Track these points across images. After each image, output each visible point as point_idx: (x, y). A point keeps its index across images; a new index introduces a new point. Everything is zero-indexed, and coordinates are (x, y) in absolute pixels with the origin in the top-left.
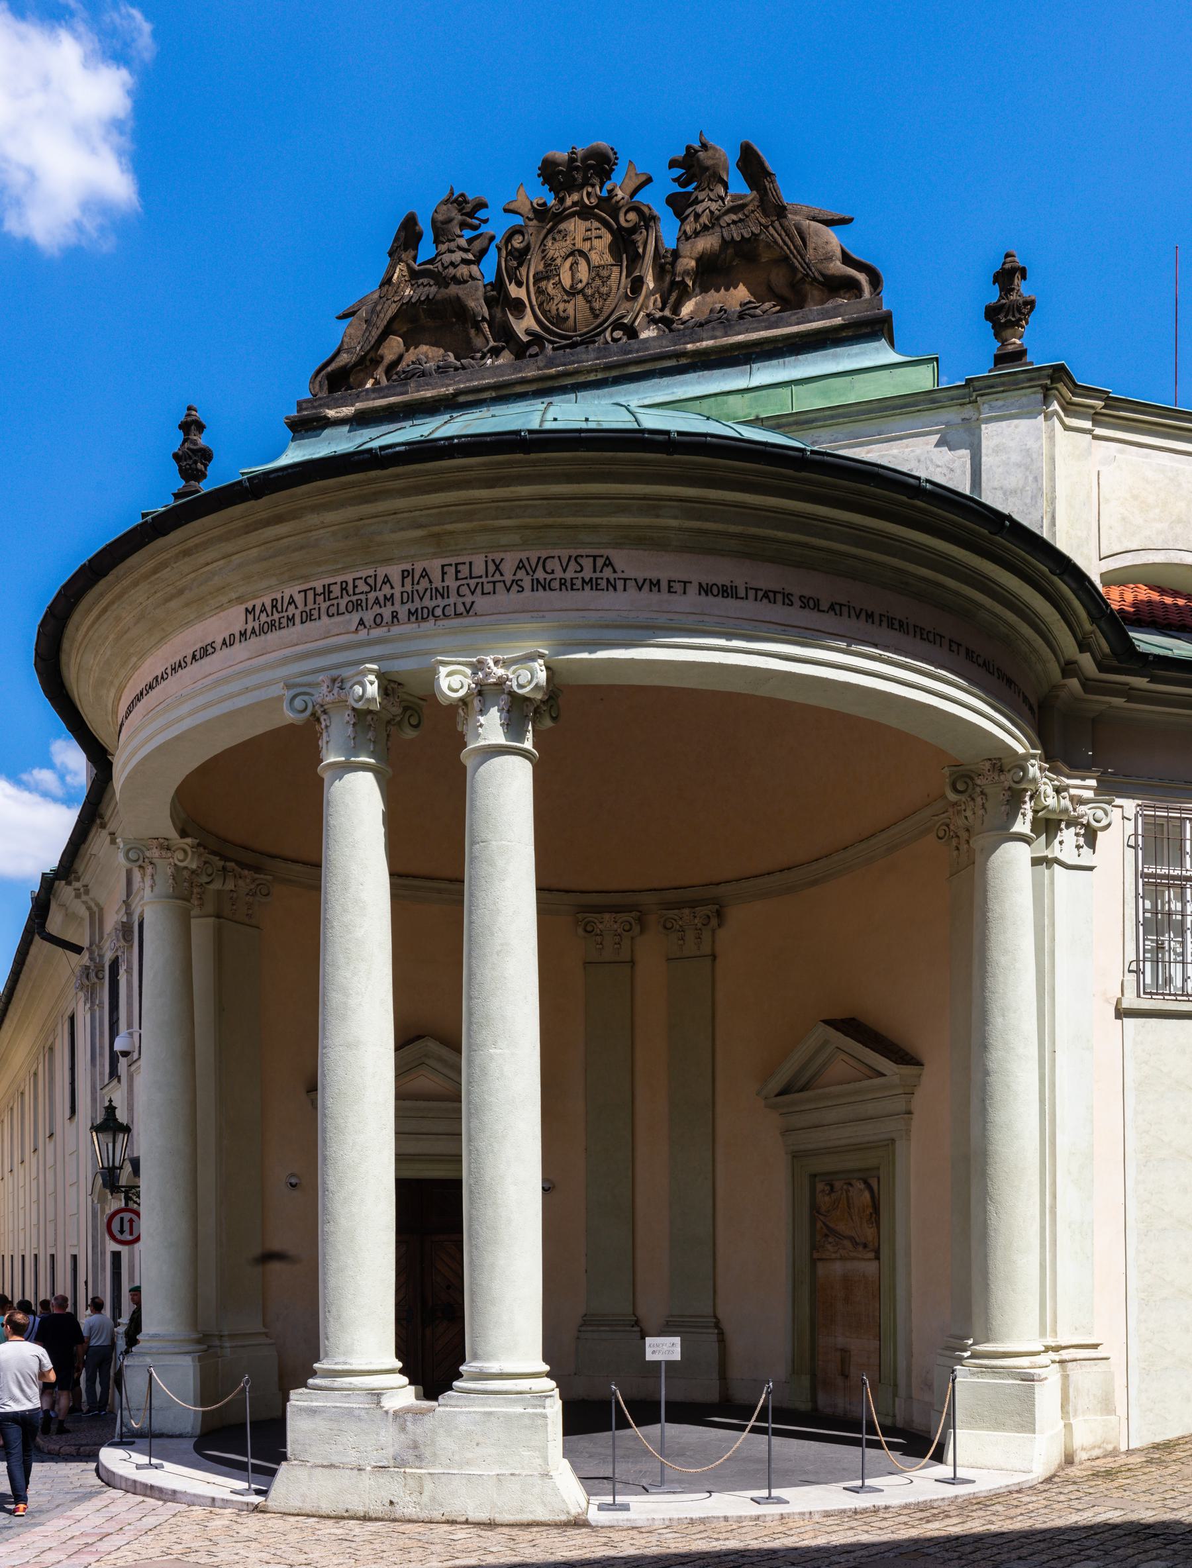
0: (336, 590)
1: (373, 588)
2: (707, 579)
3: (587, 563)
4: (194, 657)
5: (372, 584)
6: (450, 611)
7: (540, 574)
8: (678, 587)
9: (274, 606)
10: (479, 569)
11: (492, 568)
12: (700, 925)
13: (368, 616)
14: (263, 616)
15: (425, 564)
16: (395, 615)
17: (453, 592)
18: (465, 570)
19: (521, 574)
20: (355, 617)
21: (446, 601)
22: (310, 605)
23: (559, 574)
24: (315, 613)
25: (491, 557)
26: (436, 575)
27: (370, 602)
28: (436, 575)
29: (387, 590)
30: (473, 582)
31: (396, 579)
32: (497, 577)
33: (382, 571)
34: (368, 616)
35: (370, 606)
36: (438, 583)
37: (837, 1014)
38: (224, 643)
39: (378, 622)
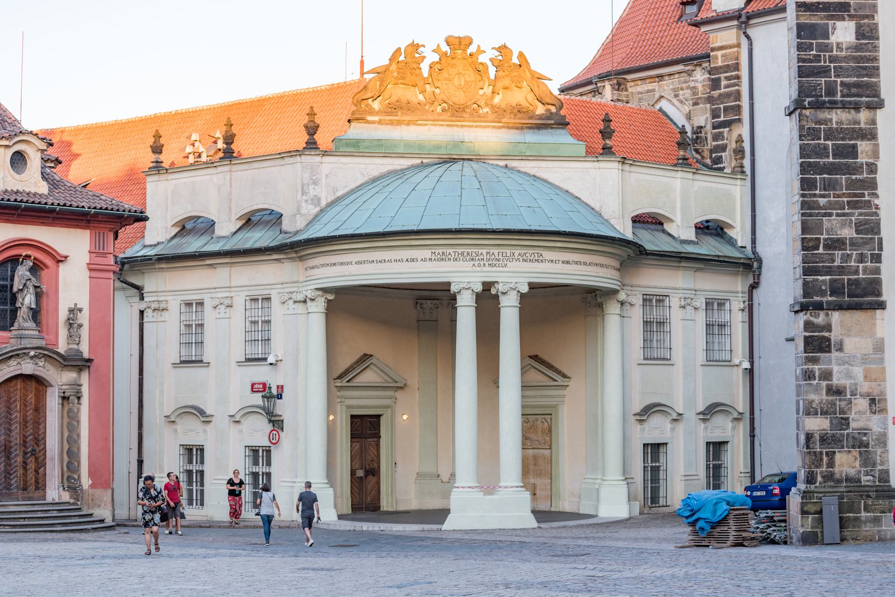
0: (465, 254)
1: (477, 255)
2: (564, 260)
3: (536, 255)
4: (407, 260)
8: (557, 262)
9: (443, 254)
10: (508, 254)
11: (512, 255)
13: (476, 263)
14: (439, 256)
16: (484, 265)
17: (501, 260)
18: (504, 255)
19: (520, 257)
20: (472, 263)
21: (499, 263)
23: (529, 258)
24: (458, 260)
26: (496, 254)
28: (496, 254)
29: (482, 256)
30: (507, 258)
31: (485, 254)
32: (513, 257)
33: (480, 251)
34: (476, 263)
36: (497, 257)
37: (532, 354)
38: (422, 260)
39: (479, 265)
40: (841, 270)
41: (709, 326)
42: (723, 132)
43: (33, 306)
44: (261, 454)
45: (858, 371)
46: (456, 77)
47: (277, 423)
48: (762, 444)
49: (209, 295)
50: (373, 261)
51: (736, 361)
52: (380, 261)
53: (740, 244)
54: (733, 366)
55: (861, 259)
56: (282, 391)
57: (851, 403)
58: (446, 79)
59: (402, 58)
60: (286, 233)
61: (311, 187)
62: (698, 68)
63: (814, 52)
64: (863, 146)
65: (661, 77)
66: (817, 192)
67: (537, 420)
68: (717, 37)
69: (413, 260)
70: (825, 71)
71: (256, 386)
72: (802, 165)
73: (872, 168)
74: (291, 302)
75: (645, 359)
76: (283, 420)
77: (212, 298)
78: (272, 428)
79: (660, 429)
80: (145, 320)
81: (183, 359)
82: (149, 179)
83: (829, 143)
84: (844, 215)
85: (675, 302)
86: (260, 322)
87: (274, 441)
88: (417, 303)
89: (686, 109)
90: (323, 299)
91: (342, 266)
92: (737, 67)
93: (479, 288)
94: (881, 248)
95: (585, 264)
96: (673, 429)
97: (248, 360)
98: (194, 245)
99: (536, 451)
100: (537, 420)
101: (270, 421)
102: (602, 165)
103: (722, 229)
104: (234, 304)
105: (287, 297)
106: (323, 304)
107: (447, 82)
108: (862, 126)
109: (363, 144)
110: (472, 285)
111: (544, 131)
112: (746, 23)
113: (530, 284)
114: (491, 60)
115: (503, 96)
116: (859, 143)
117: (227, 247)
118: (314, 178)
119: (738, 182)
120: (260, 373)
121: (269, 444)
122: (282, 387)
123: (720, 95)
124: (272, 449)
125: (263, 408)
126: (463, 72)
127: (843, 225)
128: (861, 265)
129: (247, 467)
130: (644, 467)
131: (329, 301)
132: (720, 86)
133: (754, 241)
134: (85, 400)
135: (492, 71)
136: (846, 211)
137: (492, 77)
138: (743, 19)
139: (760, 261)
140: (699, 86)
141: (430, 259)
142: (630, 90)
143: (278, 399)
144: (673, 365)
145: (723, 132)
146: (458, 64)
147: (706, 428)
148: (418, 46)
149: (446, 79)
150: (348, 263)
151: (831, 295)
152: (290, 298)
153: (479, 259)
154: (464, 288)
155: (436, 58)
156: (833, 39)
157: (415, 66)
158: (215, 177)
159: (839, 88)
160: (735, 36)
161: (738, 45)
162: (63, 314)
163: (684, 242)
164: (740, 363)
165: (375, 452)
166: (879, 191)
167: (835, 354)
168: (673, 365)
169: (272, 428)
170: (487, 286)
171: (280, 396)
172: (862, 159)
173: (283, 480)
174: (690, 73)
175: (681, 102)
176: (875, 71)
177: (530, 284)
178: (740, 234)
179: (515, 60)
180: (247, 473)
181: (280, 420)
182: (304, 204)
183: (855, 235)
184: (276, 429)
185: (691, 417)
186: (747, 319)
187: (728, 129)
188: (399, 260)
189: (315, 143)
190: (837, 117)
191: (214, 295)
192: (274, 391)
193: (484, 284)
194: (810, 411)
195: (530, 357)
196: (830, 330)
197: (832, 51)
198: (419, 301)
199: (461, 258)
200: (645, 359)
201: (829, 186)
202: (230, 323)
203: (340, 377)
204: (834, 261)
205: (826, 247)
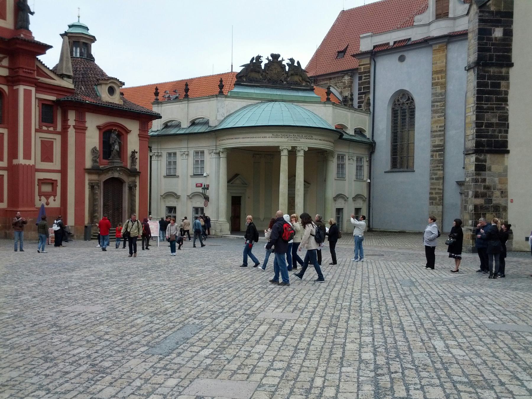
39: (290, 140)
40: (492, 136)
41: (357, 166)
43: (118, 150)
45: (496, 179)
47: (207, 198)
51: (365, 179)
53: (368, 137)
55: (500, 132)
57: (493, 193)
58: (271, 70)
59: (254, 61)
60: (211, 127)
62: (346, 75)
63: (485, 41)
64: (503, 83)
65: (330, 79)
66: (483, 102)
70: (489, 50)
72: (477, 90)
73: (506, 93)
74: (213, 154)
75: (337, 178)
80: (152, 159)
81: (168, 174)
82: (153, 106)
83: (489, 81)
84: (493, 113)
85: (347, 157)
89: (340, 90)
92: (369, 72)
93: (290, 149)
94: (508, 127)
95: (326, 141)
96: (345, 203)
98: (173, 131)
102: (327, 105)
103: (361, 132)
105: (211, 151)
108: (503, 74)
110: (287, 148)
111: (305, 92)
112: (374, 55)
113: (308, 148)
114: (287, 64)
116: (501, 82)
117: (187, 132)
119: (368, 115)
120: (200, 180)
122: (209, 185)
123: (362, 82)
125: (202, 193)
127: (493, 117)
128: (500, 134)
133: (373, 136)
134: (138, 188)
135: (287, 68)
136: (495, 111)
137: (287, 70)
138: (373, 53)
139: (375, 143)
140: (346, 81)
142: (318, 83)
147: (355, 203)
148: (260, 57)
150: (238, 138)
151: (487, 147)
152: (213, 152)
154: (284, 149)
155: (267, 62)
156: (493, 36)
157: (259, 64)
159: (495, 57)
161: (370, 64)
162: (129, 153)
163: (351, 135)
164: (367, 180)
166: (509, 103)
167: (487, 172)
170: (294, 148)
172: (503, 89)
174: (343, 77)
175: (338, 87)
176: (510, 50)
177: (308, 148)
178: (368, 134)
179: (296, 64)
182: (218, 116)
183: (498, 122)
185: (350, 199)
186: (368, 165)
189: (223, 92)
190: (492, 70)
191: (181, 150)
193: (292, 147)
194: (476, 195)
196: (486, 162)
197: (492, 41)
200: (337, 178)
201: (488, 100)
204: (489, 132)
205: (486, 126)
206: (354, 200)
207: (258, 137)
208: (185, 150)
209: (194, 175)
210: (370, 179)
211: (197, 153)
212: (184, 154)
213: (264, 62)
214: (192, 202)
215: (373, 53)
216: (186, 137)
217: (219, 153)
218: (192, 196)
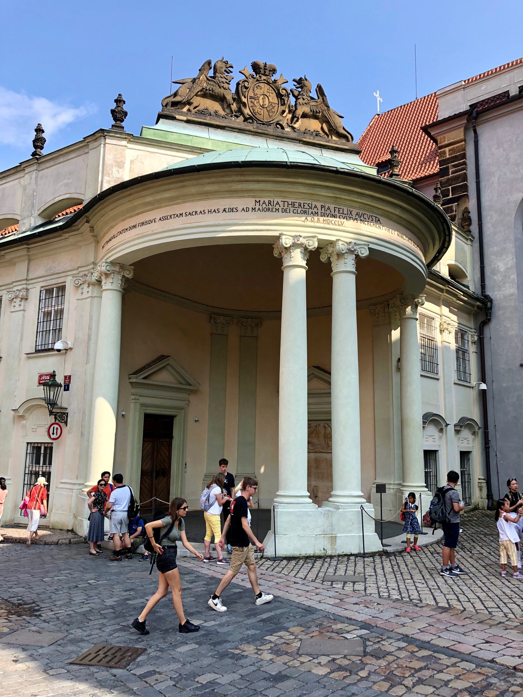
0: (297, 205)
1: (311, 208)
3: (374, 218)
4: (224, 210)
5: (311, 206)
6: (336, 223)
7: (362, 218)
9: (270, 203)
10: (345, 212)
12: (254, 325)
14: (264, 206)
15: (329, 205)
18: (341, 211)
19: (357, 217)
22: (286, 207)
24: (288, 211)
25: (349, 209)
27: (310, 213)
28: (333, 210)
30: (344, 215)
31: (319, 208)
32: (351, 216)
33: (314, 203)
35: (310, 213)
36: (333, 213)
38: (243, 209)
42: (452, 206)
44: (42, 452)
46: (262, 97)
48: (498, 454)
49: (5, 292)
50: (181, 215)
52: (190, 214)
54: (470, 387)
56: (70, 382)
61: (114, 169)
67: (319, 425)
68: (444, 138)
69: (232, 210)
71: (43, 378)
74: (86, 285)
76: (67, 413)
77: (8, 292)
78: (53, 421)
79: (433, 437)
86: (53, 311)
87: (55, 436)
88: (211, 317)
90: (120, 277)
91: (144, 227)
92: (464, 156)
93: (314, 245)
96: (440, 438)
97: (37, 351)
99: (318, 454)
100: (319, 425)
101: (51, 413)
104: (30, 297)
106: (120, 282)
107: (253, 100)
109: (171, 136)
112: (476, 118)
115: (302, 123)
118: (118, 160)
119: (469, 242)
121: (49, 441)
122: (70, 377)
123: (448, 179)
124: (54, 446)
126: (268, 95)
129: (27, 466)
130: (425, 472)
131: (125, 280)
132: (449, 172)
133: (483, 287)
135: (292, 100)
138: (474, 114)
139: (491, 301)
141: (254, 209)
143: (65, 390)
144: (438, 379)
145: (452, 206)
146: (263, 87)
149: (251, 98)
150: (151, 221)
153: (312, 213)
158: (22, 180)
160: (463, 133)
165: (167, 453)
168: (438, 379)
169: (53, 421)
171: (67, 388)
173: (63, 481)
180: (27, 472)
181: (64, 413)
184: (57, 422)
185: (451, 429)
187: (456, 203)
188: (215, 211)
192: (60, 379)
193: (319, 241)
195: (314, 367)
198: (213, 316)
199: (292, 209)
202: (24, 316)
203: (135, 373)
206: (457, 432)
207: (210, 211)
208: (19, 288)
209: (37, 351)
210: (483, 379)
211: (49, 291)
212: (16, 297)
213: (236, 77)
214: (24, 427)
215: (474, 114)
216: (21, 251)
217: (99, 282)
218: (28, 410)
